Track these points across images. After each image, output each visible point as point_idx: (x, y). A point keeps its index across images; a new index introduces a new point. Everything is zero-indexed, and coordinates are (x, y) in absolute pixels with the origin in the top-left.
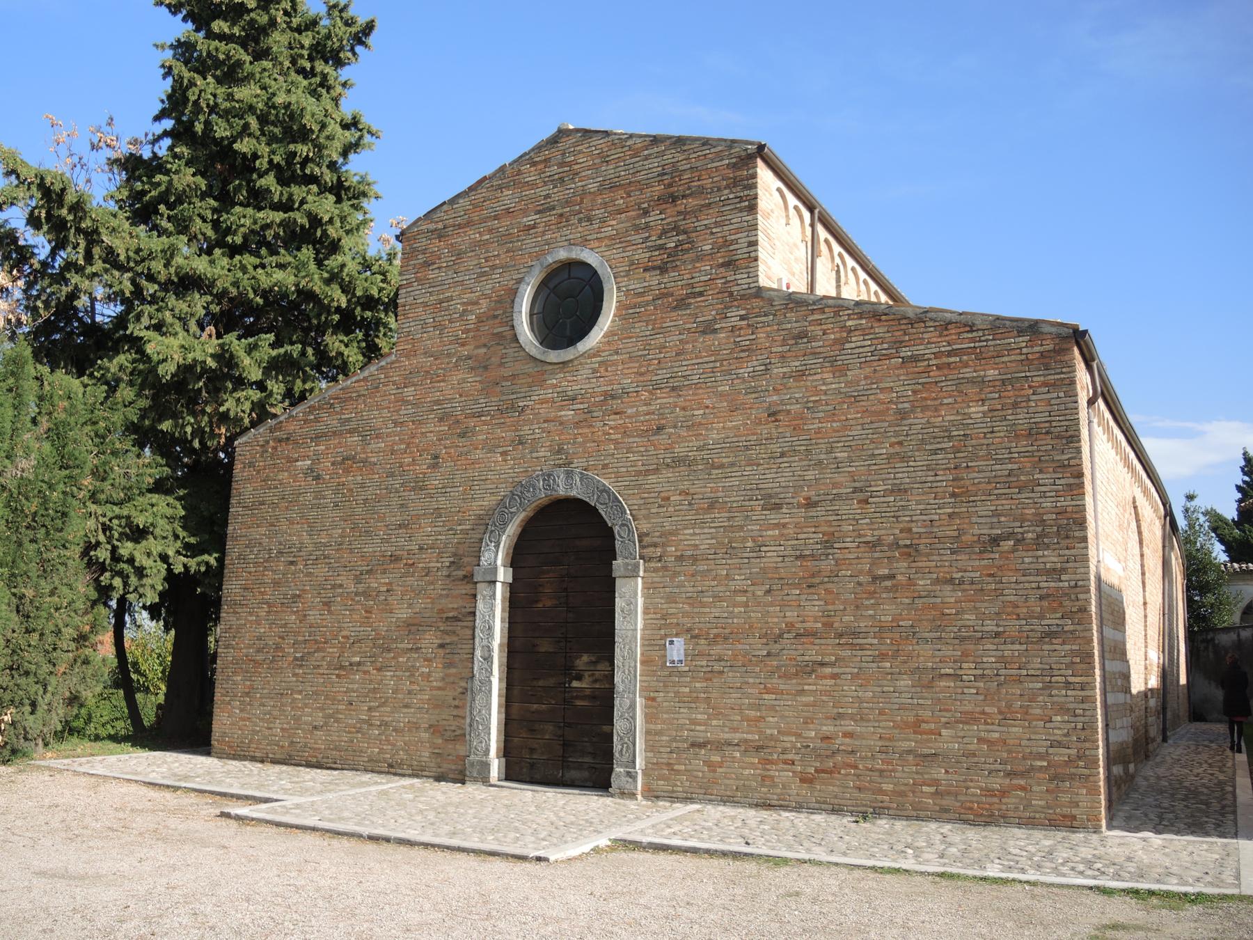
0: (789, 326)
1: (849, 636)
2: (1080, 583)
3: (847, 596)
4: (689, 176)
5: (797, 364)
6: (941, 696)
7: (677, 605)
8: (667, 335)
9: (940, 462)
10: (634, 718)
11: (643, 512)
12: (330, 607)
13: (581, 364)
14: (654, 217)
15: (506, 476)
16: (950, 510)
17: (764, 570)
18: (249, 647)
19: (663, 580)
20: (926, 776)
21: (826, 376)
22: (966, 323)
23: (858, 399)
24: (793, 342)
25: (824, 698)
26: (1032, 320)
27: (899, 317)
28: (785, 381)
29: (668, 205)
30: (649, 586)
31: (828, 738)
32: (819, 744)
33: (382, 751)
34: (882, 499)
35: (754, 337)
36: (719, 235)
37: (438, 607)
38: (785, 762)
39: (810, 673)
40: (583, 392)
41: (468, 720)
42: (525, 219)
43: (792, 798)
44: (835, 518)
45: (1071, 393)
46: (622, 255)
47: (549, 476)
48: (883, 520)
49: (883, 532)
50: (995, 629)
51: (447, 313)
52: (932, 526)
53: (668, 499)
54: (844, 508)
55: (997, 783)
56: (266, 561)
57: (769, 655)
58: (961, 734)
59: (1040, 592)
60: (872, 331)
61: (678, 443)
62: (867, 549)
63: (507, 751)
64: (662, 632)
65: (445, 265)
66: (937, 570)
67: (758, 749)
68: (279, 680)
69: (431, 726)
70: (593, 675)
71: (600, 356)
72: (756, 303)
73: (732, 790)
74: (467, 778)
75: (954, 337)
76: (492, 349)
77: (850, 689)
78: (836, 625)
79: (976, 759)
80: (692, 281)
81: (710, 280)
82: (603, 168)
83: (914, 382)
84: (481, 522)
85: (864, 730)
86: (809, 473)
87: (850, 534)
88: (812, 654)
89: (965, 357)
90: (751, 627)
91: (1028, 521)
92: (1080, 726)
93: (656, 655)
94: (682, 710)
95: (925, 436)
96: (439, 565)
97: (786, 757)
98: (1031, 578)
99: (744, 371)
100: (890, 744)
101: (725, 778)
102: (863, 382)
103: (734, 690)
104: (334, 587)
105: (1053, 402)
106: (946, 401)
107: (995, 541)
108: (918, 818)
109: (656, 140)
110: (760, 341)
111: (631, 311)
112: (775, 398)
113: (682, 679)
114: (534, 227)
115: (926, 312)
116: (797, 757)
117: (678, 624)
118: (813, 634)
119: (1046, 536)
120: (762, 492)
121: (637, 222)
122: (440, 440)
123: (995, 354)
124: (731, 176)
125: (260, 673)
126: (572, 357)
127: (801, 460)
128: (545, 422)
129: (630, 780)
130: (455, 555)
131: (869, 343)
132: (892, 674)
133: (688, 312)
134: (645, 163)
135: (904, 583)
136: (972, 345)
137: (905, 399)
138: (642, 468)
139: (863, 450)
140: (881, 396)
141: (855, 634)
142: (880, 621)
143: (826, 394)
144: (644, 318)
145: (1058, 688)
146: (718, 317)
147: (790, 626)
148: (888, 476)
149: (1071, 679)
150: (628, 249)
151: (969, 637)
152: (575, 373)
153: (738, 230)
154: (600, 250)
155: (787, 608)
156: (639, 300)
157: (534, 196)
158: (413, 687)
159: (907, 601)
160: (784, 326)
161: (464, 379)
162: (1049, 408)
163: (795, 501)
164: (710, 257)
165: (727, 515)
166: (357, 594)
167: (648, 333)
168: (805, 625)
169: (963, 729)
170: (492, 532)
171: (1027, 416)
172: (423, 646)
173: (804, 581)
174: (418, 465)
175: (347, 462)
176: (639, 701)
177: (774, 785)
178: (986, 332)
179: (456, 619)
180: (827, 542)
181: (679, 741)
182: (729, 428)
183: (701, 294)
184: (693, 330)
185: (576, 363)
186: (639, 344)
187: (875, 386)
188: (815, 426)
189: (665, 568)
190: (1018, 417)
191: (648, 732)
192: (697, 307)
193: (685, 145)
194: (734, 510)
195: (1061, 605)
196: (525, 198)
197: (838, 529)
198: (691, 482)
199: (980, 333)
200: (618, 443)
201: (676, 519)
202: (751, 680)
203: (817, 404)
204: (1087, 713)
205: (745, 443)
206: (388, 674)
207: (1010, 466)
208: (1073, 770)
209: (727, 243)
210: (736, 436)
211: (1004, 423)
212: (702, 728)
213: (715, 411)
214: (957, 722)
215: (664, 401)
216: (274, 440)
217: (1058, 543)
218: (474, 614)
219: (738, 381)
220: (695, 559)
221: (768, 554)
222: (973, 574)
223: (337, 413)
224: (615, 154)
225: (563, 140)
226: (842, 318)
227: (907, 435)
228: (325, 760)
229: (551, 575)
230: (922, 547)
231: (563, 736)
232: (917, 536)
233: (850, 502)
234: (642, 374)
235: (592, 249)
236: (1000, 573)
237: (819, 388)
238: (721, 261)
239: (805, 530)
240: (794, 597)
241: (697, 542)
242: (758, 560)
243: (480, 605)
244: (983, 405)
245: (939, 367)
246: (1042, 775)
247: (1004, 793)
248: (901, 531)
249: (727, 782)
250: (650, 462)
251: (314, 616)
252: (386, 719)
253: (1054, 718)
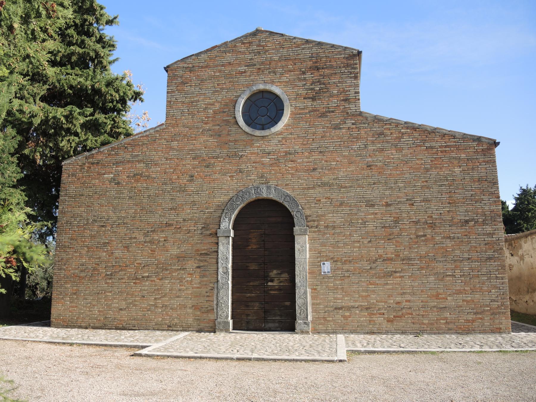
0: (375, 129)
2: (500, 239)
3: (406, 243)
4: (325, 60)
5: (380, 145)
6: (447, 283)
7: (326, 248)
8: (316, 128)
9: (443, 190)
10: (306, 298)
11: (307, 206)
12: (129, 249)
13: (272, 138)
14: (308, 75)
15: (233, 187)
16: (448, 209)
17: (367, 233)
18: (76, 269)
19: (318, 236)
20: (442, 316)
21: (393, 151)
22: (452, 135)
23: (408, 162)
24: (378, 136)
25: (397, 286)
26: (478, 136)
27: (424, 130)
28: (374, 152)
29: (315, 71)
30: (311, 239)
31: (399, 303)
32: (395, 306)
33: (163, 319)
34: (419, 204)
35: (359, 132)
36: (341, 87)
37: (195, 248)
38: (380, 314)
39: (390, 276)
40: (274, 150)
41: (215, 302)
42: (239, 68)
43: (383, 329)
44: (399, 211)
45: (494, 166)
46: (292, 90)
47: (258, 188)
48: (420, 212)
49: (420, 217)
50: (468, 256)
51: (196, 108)
52: (441, 215)
53: (320, 200)
54: (403, 207)
55: (470, 317)
56: (86, 225)
57: (371, 268)
58: (456, 298)
59: (485, 242)
60: (413, 135)
61: (324, 176)
62: (414, 224)
64: (319, 259)
65: (194, 84)
66: (444, 233)
67: (367, 309)
68: (96, 286)
69: (193, 306)
70: (279, 279)
71: (283, 135)
72: (360, 118)
73: (355, 327)
74: (216, 330)
75: (447, 140)
76: (222, 127)
77: (408, 282)
78: (401, 256)
79: (462, 308)
80: (328, 106)
81: (337, 106)
82: (281, 50)
83: (431, 157)
84: (220, 208)
85: (414, 299)
86: (387, 192)
87: (406, 218)
88: (390, 268)
89: (452, 149)
90: (362, 257)
91: (480, 214)
92: (502, 293)
93: (316, 270)
94: (330, 294)
95: (437, 179)
96: (196, 228)
97: (380, 311)
98: (482, 237)
99: (355, 147)
100: (427, 304)
101: (352, 322)
102: (409, 155)
103: (356, 284)
104: (131, 238)
105: (487, 168)
106: (445, 165)
107: (467, 222)
108: (439, 333)
109: (308, 42)
110: (362, 134)
111: (298, 116)
112: (370, 159)
113: (329, 280)
114: (245, 72)
115: (436, 129)
116: (385, 312)
117: (326, 256)
118: (391, 259)
119: (487, 220)
120: (365, 199)
121: (300, 77)
122: (194, 168)
123: (464, 148)
124: (346, 62)
125: (84, 283)
126: (268, 134)
127: (383, 186)
128: (254, 163)
129: (306, 326)
130: (205, 224)
131: (411, 139)
132: (426, 275)
133: (327, 119)
134: (303, 51)
135: (430, 238)
136: (455, 144)
137: (428, 164)
138: (306, 186)
139: (410, 183)
140: (417, 162)
141: (410, 259)
142: (420, 254)
143: (393, 159)
144: (305, 120)
145: (493, 279)
146: (341, 123)
147: (380, 256)
148: (422, 195)
149: (498, 276)
150: (296, 88)
151: (458, 260)
152: (269, 142)
153: (350, 86)
154: (281, 87)
155: (378, 249)
156: (302, 111)
157: (244, 58)
158: (182, 288)
159: (431, 245)
160: (373, 129)
161: (208, 140)
162: (486, 171)
163: (381, 203)
164: (336, 96)
165: (349, 208)
166: (145, 242)
167: (307, 126)
168: (387, 256)
169: (456, 297)
170: (226, 213)
171: (478, 173)
172: (187, 267)
173: (386, 237)
174: (181, 179)
175: (137, 176)
176: (309, 290)
177: (376, 324)
178: (460, 139)
179: (206, 254)
180: (396, 221)
181: (329, 307)
182: (349, 171)
183: (333, 112)
184: (330, 127)
185: (269, 137)
186: (303, 131)
187: (415, 157)
188: (389, 172)
189: (319, 231)
190: (474, 173)
191: (313, 304)
192: (331, 117)
193: (322, 46)
194: (353, 206)
195: (493, 247)
196: (239, 58)
197: (400, 216)
198: (331, 194)
199: (458, 140)
200: (293, 175)
201: (324, 209)
202: (363, 280)
203: (389, 163)
204: (504, 288)
205: (356, 178)
206: (166, 281)
207: (472, 193)
208: (500, 310)
209: (345, 91)
210: (352, 175)
211: (469, 176)
212: (340, 301)
213: (342, 163)
214: (453, 294)
215: (317, 157)
216: (89, 163)
217: (491, 223)
218: (217, 252)
219: (352, 151)
220: (334, 228)
221: (369, 226)
222: (458, 235)
223: (130, 152)
224: (287, 44)
225: (259, 34)
226: (399, 128)
227: (429, 178)
228: (128, 326)
229: (255, 234)
230: (437, 224)
231: (264, 308)
232: (435, 219)
233: (405, 205)
234: (304, 145)
236: (469, 235)
237: (390, 156)
238: (342, 98)
239: (386, 216)
240: (382, 244)
241: (335, 220)
242: (364, 228)
243: (221, 247)
244: (460, 168)
245: (442, 152)
246: (488, 313)
247: (473, 321)
248: (428, 217)
249: (353, 324)
250: (310, 184)
251: (118, 253)
252: (166, 303)
253: (492, 291)
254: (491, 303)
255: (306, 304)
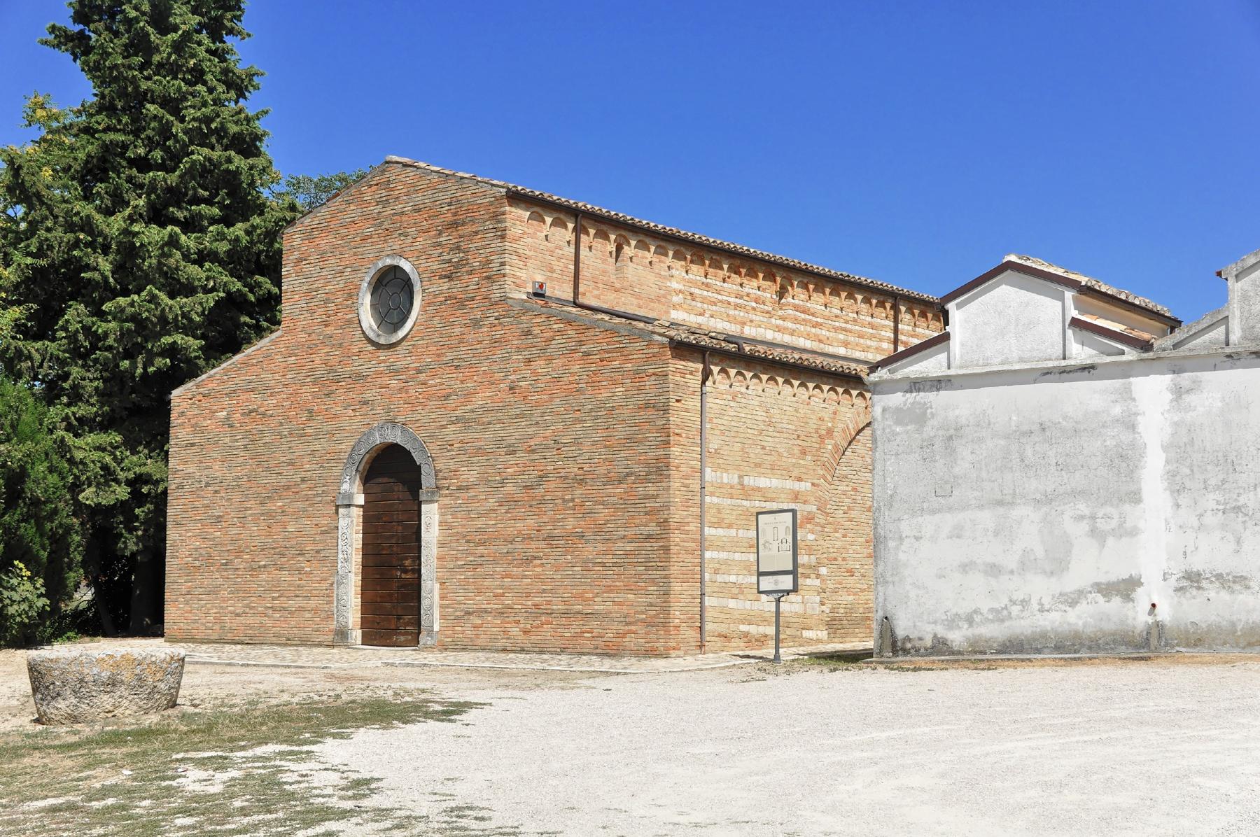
1: (550, 538)
55: (622, 629)
63: (365, 624)
141: (553, 538)
191: (441, 607)
220: (467, 488)
235: (407, 259)
247: (624, 635)
254: (647, 608)
255: (431, 607)
